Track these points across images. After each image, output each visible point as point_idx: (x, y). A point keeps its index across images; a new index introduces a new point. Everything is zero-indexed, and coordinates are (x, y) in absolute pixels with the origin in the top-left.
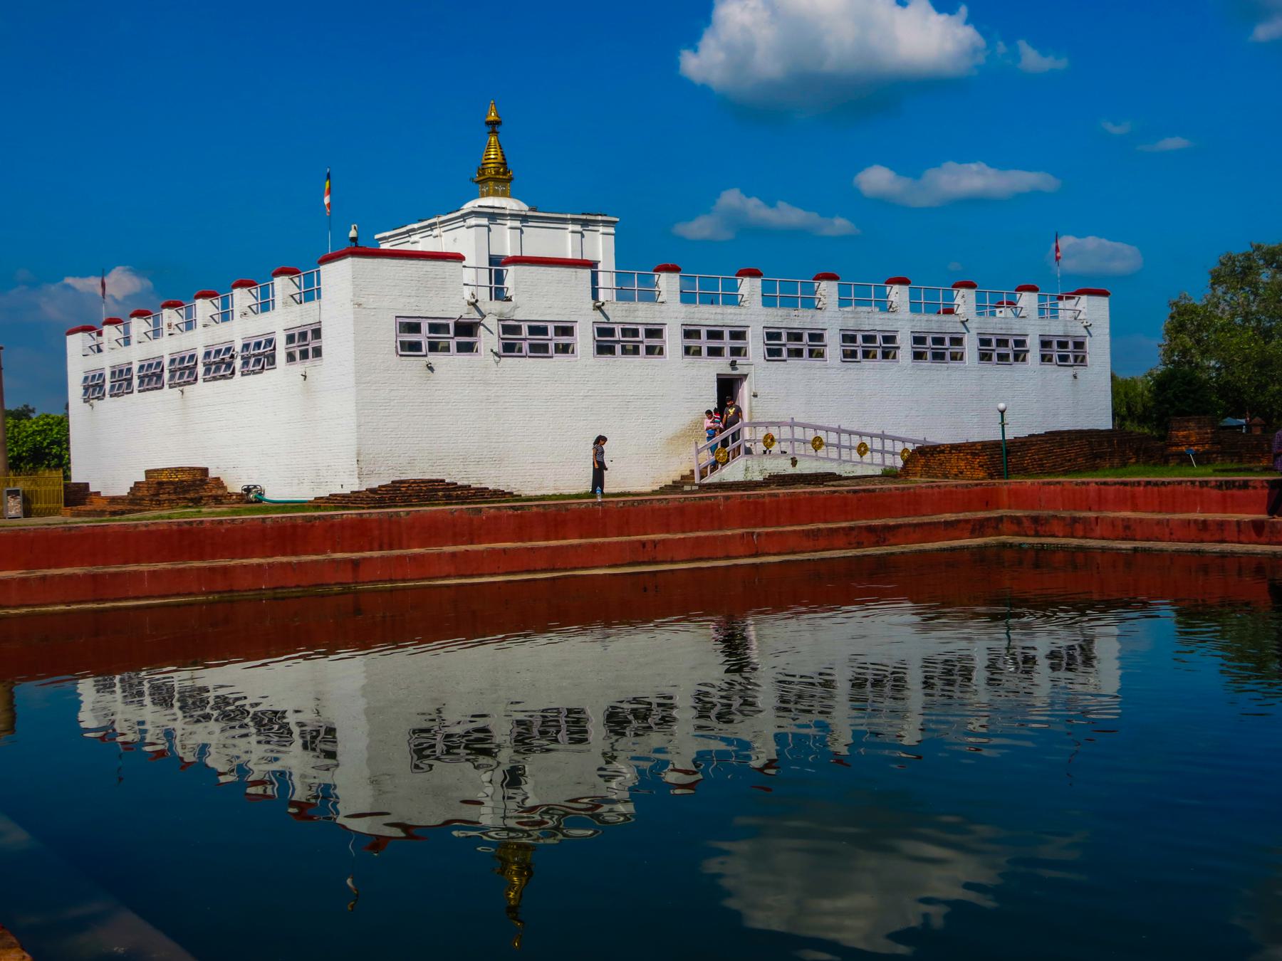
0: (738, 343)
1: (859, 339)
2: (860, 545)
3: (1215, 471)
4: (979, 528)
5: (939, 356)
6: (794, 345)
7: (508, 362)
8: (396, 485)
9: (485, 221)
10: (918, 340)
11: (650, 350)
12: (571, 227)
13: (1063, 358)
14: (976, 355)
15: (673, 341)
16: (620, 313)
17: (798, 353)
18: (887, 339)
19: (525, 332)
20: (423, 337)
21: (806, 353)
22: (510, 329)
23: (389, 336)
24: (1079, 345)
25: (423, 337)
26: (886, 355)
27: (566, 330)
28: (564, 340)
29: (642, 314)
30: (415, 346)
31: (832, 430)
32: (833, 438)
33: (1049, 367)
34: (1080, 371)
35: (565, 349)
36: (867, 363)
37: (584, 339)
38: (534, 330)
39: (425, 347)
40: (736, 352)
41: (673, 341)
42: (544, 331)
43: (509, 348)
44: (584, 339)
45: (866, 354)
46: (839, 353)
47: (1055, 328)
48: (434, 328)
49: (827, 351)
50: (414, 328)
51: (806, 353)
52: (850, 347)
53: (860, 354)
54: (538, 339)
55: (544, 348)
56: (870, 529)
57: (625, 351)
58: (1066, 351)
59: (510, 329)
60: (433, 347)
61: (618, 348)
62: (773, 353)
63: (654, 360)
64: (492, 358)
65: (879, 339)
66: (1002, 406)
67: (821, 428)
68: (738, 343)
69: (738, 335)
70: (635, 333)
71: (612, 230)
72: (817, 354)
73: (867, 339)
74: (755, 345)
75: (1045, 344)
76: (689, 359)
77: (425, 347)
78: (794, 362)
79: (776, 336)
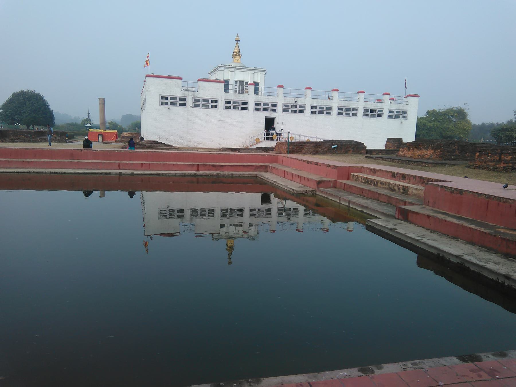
0: (274, 108)
1: (318, 108)
2: (209, 170)
3: (366, 157)
4: (257, 168)
5: (347, 114)
6: (294, 109)
7: (196, 109)
8: (156, 142)
9: (223, 69)
10: (340, 109)
11: (243, 109)
12: (251, 72)
13: (398, 117)
14: (362, 114)
15: (251, 106)
16: (231, 96)
17: (295, 111)
18: (328, 108)
19: (201, 101)
20: (169, 101)
21: (298, 111)
22: (195, 100)
23: (158, 100)
24: (405, 113)
25: (169, 101)
26: (328, 113)
27: (216, 102)
28: (214, 104)
29: (241, 98)
30: (166, 104)
31: (298, 135)
32: (298, 137)
33: (391, 120)
34: (404, 121)
35: (216, 107)
36: (320, 115)
37: (221, 104)
38: (205, 101)
39: (169, 104)
40: (275, 110)
41: (251, 106)
42: (207, 101)
43: (196, 106)
44: (221, 104)
45: (321, 113)
46: (309, 112)
47: (395, 107)
48: (172, 99)
49: (305, 111)
50: (166, 98)
51: (298, 111)
52: (314, 110)
53: (317, 112)
54: (206, 103)
55: (207, 106)
56: (213, 166)
57: (235, 108)
58: (399, 115)
59: (195, 100)
60: (172, 104)
61: (232, 108)
62: (285, 111)
63: (244, 112)
64: (190, 109)
65: (325, 108)
66: (289, 130)
67: (294, 134)
68: (274, 108)
69: (275, 105)
70: (239, 103)
71: (264, 73)
72: (301, 112)
73: (320, 108)
74: (280, 108)
75: (390, 112)
76: (257, 111)
77: (169, 104)
78: (293, 114)
79: (288, 106)
